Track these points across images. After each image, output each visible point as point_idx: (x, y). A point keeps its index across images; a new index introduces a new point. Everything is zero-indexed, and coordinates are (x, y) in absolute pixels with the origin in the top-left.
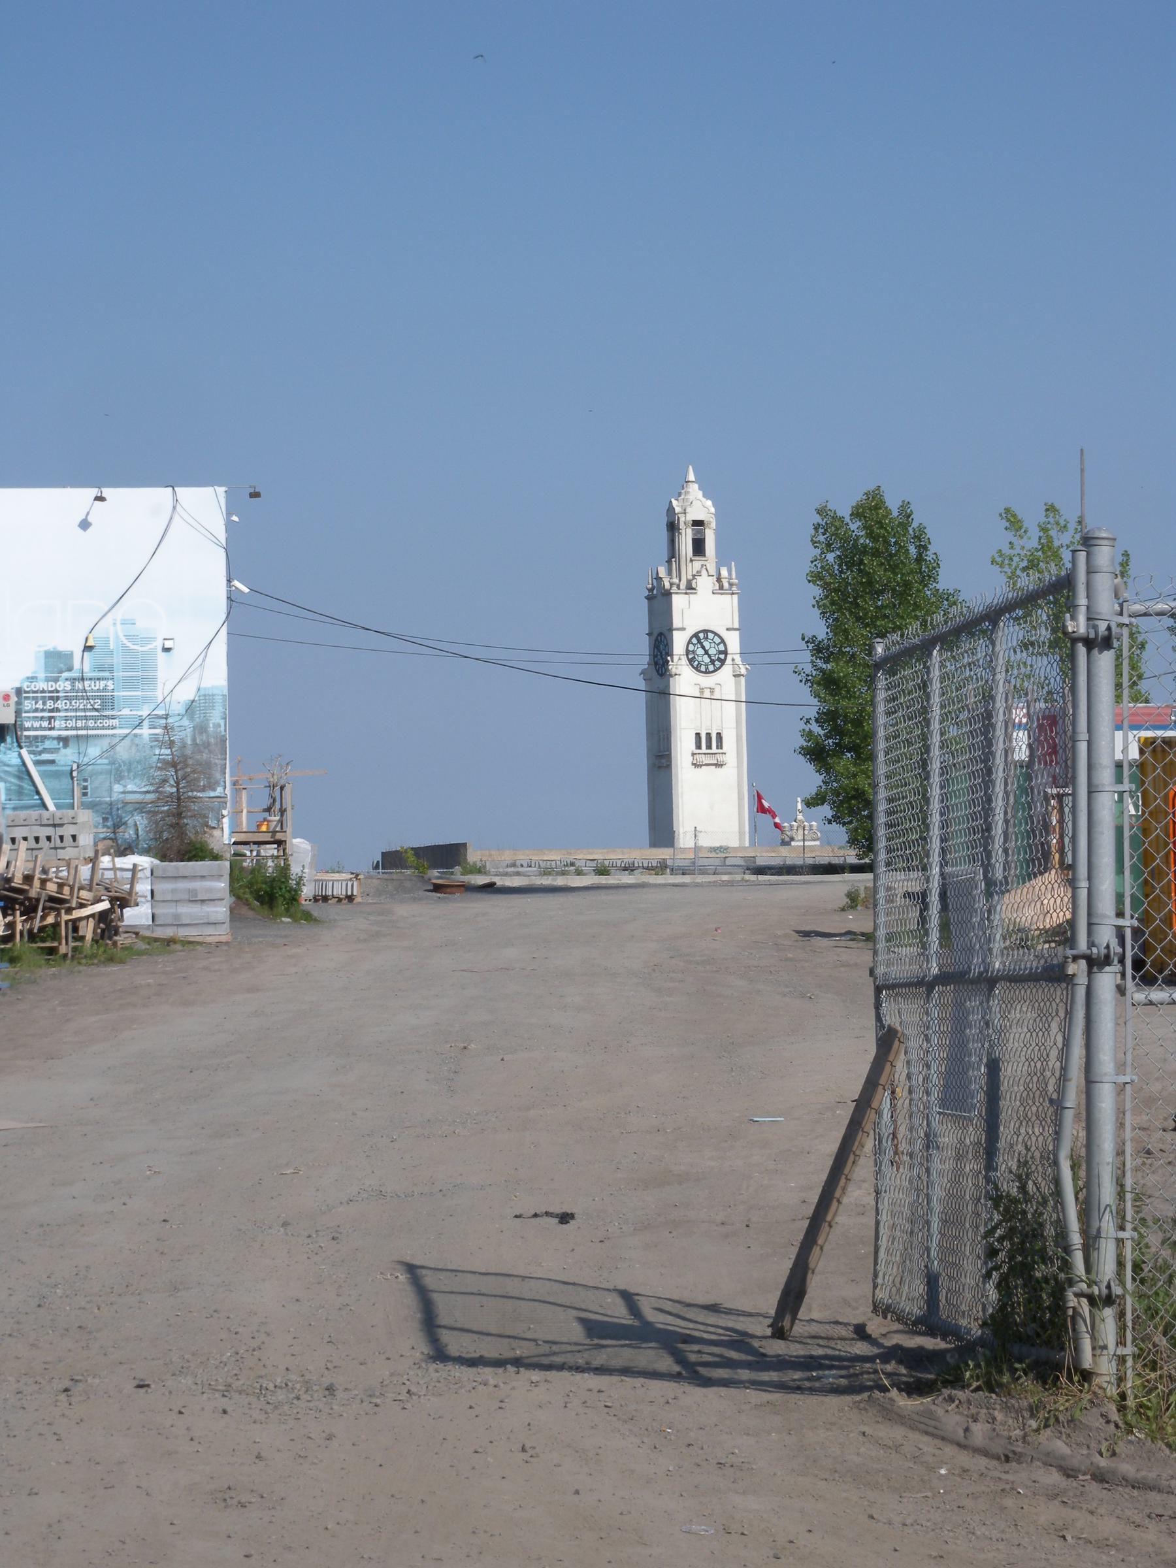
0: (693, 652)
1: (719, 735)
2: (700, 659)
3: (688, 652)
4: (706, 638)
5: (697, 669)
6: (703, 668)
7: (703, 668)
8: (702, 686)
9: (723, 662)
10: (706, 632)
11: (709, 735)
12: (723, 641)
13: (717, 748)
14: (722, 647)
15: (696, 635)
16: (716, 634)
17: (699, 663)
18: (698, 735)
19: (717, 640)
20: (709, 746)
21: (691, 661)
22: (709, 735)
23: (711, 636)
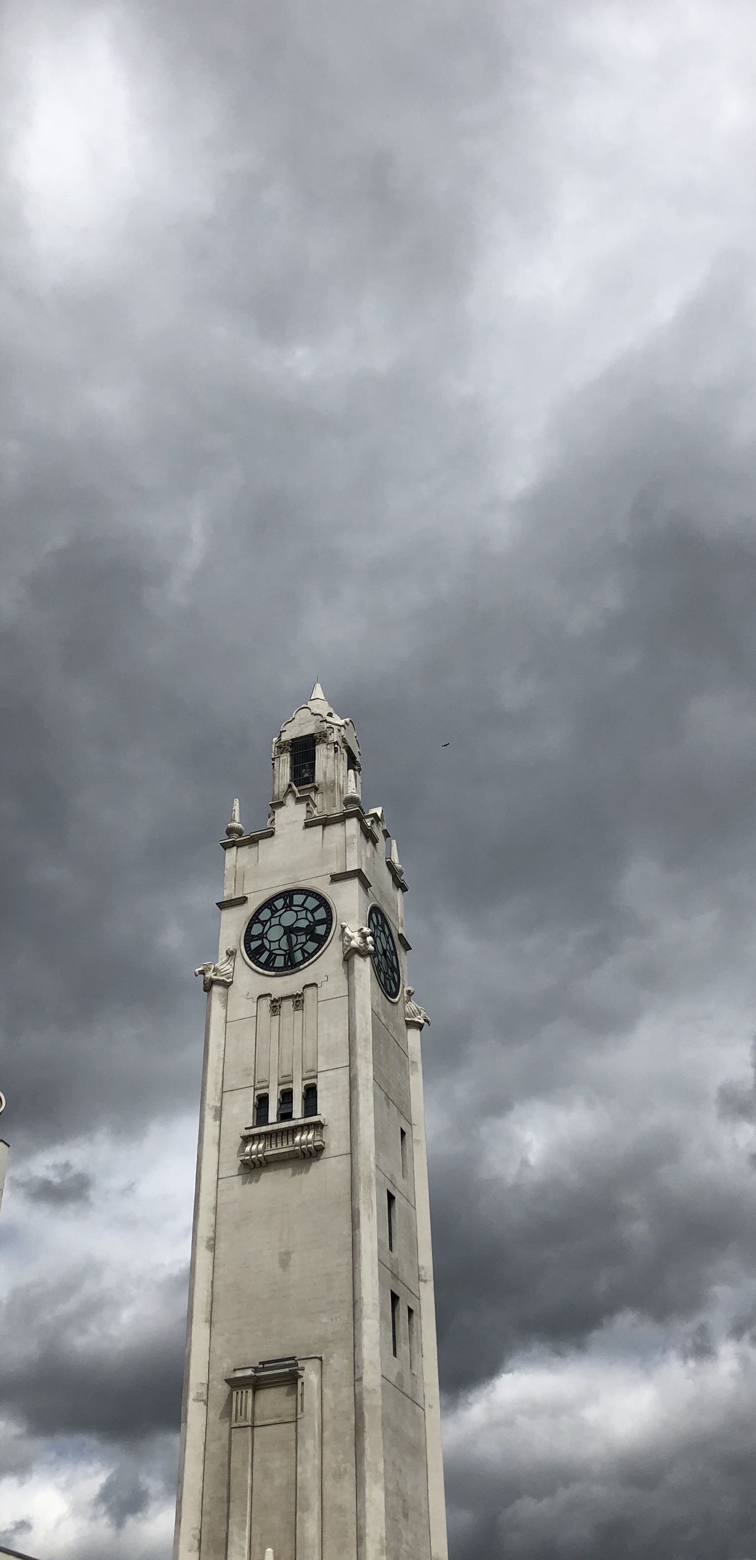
0: (262, 936)
1: (311, 1092)
2: (274, 946)
3: (249, 938)
5: (266, 966)
7: (280, 962)
8: (275, 996)
9: (321, 940)
10: (287, 895)
11: (286, 1096)
13: (306, 1115)
14: (321, 914)
15: (269, 904)
16: (308, 893)
18: (262, 1102)
19: (312, 903)
20: (285, 1116)
21: (254, 955)
22: (286, 1096)
23: (298, 899)
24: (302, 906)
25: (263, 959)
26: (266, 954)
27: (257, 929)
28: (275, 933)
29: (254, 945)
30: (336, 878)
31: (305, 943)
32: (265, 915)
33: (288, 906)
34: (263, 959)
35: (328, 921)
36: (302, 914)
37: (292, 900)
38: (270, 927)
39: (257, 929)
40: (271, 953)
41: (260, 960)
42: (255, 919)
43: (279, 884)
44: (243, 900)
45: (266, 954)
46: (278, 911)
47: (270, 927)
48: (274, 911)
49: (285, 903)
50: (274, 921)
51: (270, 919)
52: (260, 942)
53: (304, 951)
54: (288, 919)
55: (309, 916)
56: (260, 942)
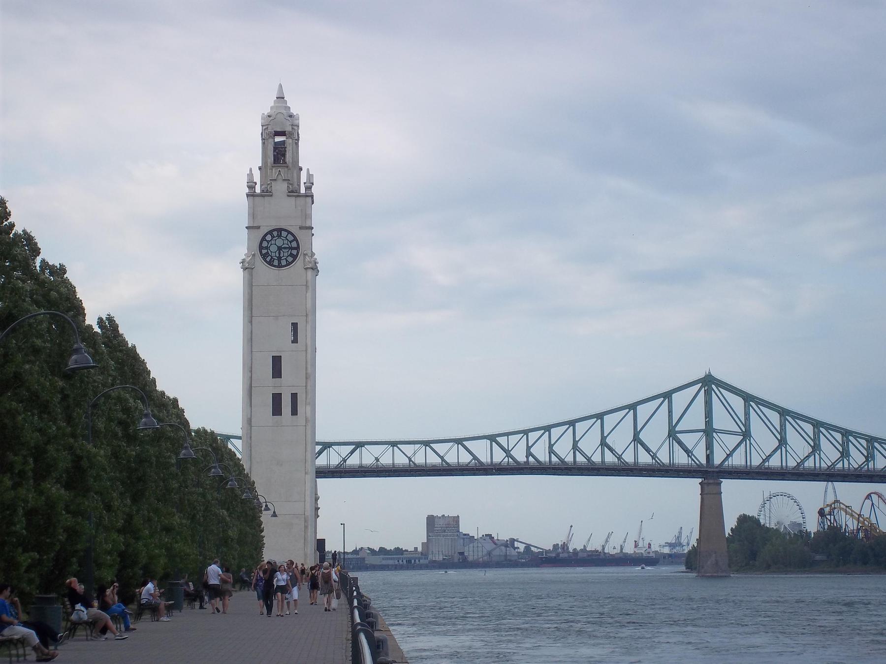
0: (267, 248)
2: (273, 254)
3: (261, 248)
4: (279, 236)
5: (270, 263)
6: (276, 263)
9: (295, 257)
10: (280, 230)
12: (295, 239)
14: (294, 244)
15: (270, 232)
16: (289, 232)
17: (272, 258)
19: (290, 238)
21: (264, 256)
23: (284, 234)
24: (286, 238)
25: (268, 259)
26: (270, 257)
27: (265, 244)
28: (273, 248)
29: (264, 251)
30: (301, 228)
31: (287, 257)
32: (269, 238)
33: (279, 236)
34: (268, 259)
35: (298, 248)
36: (286, 242)
37: (281, 234)
38: (271, 244)
39: (265, 244)
40: (272, 258)
41: (267, 259)
42: (264, 239)
43: (274, 224)
44: (258, 228)
45: (270, 257)
46: (274, 237)
47: (271, 244)
48: (273, 237)
49: (278, 234)
50: (273, 242)
51: (271, 240)
52: (266, 251)
53: (287, 261)
54: (279, 242)
55: (289, 243)
56: (266, 251)
